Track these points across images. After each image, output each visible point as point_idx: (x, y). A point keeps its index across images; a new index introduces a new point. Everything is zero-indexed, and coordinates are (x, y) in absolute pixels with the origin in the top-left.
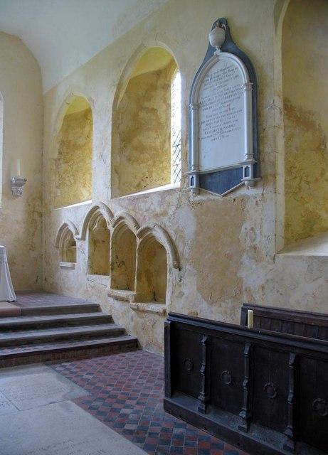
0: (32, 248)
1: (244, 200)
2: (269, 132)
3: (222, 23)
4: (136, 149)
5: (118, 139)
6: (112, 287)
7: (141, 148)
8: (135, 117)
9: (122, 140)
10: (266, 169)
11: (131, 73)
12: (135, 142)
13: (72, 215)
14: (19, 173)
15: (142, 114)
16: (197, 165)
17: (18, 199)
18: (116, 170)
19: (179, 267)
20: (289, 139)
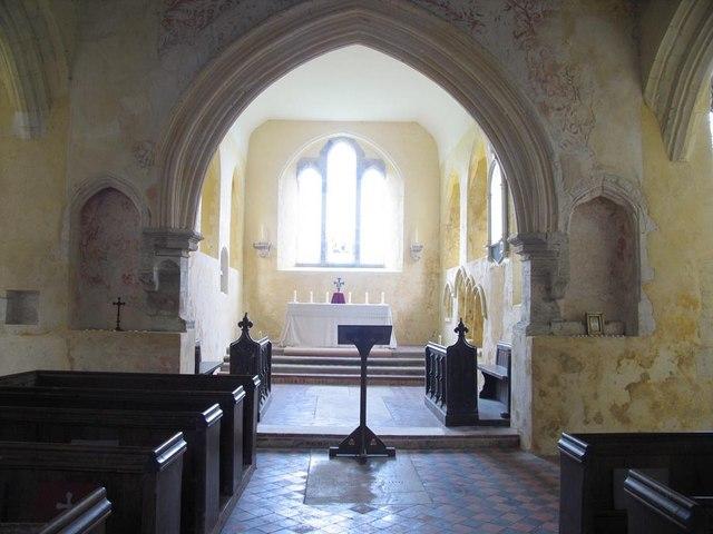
0: (430, 306)
5: (472, 214)
9: (475, 213)
13: (450, 278)
14: (417, 240)
17: (419, 263)
18: (470, 239)
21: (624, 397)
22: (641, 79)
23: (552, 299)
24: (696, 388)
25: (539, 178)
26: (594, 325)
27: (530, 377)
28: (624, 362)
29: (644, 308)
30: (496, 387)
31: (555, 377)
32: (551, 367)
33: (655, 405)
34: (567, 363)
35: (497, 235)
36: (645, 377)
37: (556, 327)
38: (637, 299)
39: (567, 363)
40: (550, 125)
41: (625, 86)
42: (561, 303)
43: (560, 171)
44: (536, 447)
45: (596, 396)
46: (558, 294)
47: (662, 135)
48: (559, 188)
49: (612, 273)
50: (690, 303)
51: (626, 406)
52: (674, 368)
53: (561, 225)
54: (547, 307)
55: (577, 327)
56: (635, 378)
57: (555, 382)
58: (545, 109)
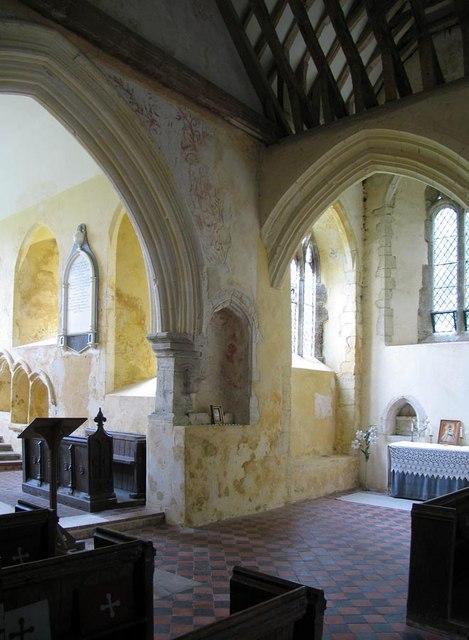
1: (90, 357)
2: (104, 313)
3: (83, 229)
4: (35, 305)
6: (12, 421)
7: (38, 305)
8: (34, 279)
10: (102, 338)
11: (30, 241)
12: (33, 300)
15: (40, 276)
16: (66, 329)
19: (55, 404)
20: (119, 317)
21: (241, 473)
22: (262, 217)
23: (188, 393)
24: (278, 463)
25: (187, 285)
26: (217, 415)
27: (182, 462)
28: (241, 445)
29: (253, 402)
30: (136, 471)
31: (200, 461)
32: (197, 452)
33: (258, 478)
34: (209, 448)
35: (81, 322)
36: (253, 456)
37: (192, 417)
38: (248, 396)
39: (209, 448)
40: (203, 237)
41: (249, 217)
42: (193, 396)
43: (206, 282)
44: (189, 521)
45: (225, 474)
46: (196, 389)
47: (269, 265)
48: (205, 295)
49: (222, 372)
50: (277, 398)
51: (242, 480)
52: (267, 449)
53: (204, 330)
54: (184, 399)
55: (205, 418)
56: (248, 458)
57: (199, 466)
58: (200, 223)
